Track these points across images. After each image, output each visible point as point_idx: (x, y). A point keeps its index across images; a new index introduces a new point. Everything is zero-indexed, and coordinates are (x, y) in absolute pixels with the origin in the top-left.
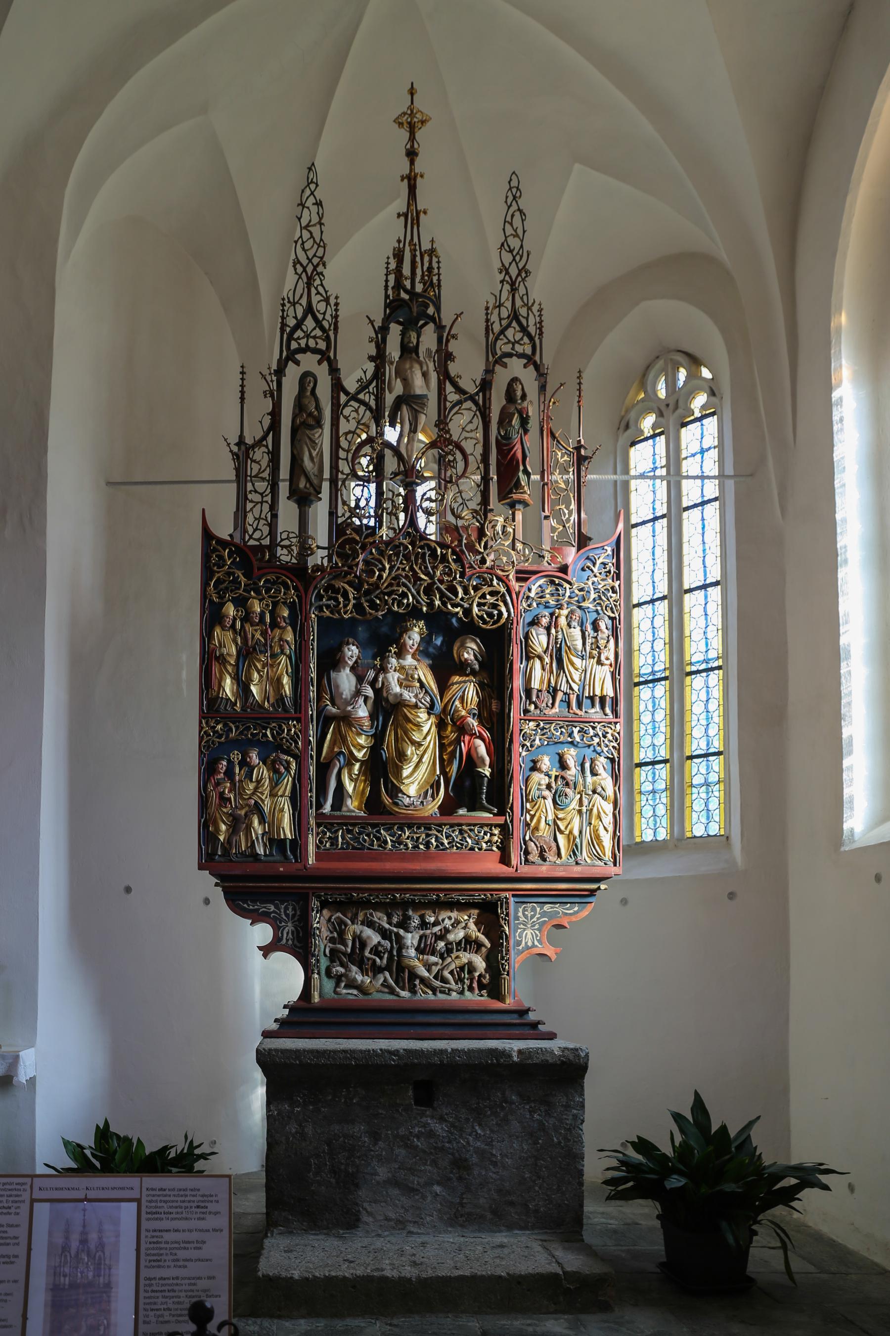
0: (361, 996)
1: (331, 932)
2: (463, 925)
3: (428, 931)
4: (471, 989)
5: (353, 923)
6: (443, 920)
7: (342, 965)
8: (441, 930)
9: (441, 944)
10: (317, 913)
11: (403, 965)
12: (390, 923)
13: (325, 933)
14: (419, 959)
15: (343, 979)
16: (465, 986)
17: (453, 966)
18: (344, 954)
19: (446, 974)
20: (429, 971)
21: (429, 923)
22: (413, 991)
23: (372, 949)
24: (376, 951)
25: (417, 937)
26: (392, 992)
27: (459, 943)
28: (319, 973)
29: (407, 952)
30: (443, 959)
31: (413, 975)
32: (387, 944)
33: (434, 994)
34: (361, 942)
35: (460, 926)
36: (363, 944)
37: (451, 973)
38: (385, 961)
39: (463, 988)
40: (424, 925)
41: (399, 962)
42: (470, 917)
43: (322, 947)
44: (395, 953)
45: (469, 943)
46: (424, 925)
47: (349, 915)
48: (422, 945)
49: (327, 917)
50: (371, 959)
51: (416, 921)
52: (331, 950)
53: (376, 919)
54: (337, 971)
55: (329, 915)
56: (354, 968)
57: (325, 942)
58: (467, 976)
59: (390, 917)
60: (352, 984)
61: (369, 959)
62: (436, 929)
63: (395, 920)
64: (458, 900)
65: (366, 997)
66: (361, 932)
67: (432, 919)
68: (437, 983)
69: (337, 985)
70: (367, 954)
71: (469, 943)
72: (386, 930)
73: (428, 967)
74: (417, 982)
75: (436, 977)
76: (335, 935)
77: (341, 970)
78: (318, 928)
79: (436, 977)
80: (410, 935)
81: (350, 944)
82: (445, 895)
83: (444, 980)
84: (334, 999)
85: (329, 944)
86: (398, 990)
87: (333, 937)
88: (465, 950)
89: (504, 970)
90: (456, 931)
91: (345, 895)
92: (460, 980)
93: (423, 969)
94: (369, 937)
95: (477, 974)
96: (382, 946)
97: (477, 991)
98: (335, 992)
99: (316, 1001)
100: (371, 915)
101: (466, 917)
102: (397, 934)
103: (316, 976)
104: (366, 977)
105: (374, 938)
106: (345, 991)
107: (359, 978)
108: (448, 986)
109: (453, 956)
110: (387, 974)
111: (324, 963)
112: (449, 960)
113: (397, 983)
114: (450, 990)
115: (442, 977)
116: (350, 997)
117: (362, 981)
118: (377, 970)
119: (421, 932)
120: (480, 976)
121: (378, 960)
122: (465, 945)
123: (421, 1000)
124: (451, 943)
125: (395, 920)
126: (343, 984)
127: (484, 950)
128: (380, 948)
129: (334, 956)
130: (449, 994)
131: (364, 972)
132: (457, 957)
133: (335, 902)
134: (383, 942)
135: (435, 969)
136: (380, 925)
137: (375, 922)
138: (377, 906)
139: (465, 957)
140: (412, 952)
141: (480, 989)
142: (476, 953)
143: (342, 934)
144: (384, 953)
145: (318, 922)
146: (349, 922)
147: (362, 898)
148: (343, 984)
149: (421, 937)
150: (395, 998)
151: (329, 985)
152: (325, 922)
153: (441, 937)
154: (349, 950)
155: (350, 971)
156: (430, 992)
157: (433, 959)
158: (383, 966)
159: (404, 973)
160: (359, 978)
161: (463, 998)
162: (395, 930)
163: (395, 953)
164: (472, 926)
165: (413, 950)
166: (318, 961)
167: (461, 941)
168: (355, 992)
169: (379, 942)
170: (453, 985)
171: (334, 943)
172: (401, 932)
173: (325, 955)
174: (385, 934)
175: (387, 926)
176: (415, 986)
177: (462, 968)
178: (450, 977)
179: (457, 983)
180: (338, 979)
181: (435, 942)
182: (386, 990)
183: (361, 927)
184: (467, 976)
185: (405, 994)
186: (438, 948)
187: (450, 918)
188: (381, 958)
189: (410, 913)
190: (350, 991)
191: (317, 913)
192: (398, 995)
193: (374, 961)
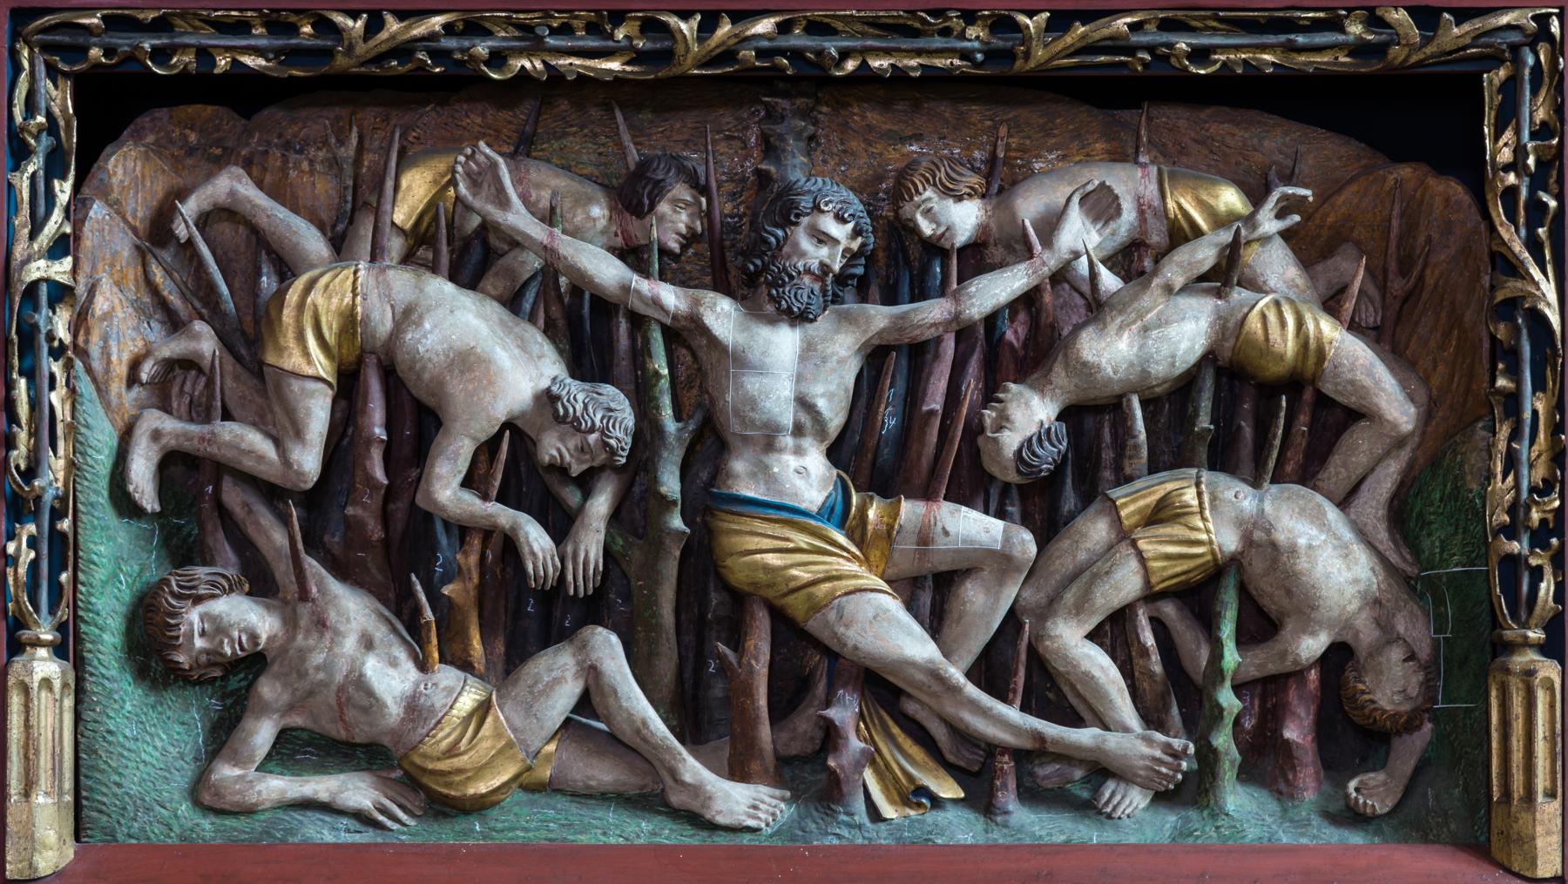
0: (406, 828)
1: (175, 324)
2: (1204, 254)
3: (934, 311)
4: (1265, 760)
5: (340, 245)
6: (1050, 225)
7: (259, 581)
8: (1028, 300)
9: (1031, 413)
10: (55, 168)
11: (738, 571)
12: (632, 255)
13: (122, 330)
14: (858, 532)
15: (268, 689)
16: (1223, 740)
17: (1125, 583)
18: (272, 493)
19: (1073, 643)
20: (935, 623)
21: (935, 249)
22: (812, 777)
23: (488, 448)
24: (513, 463)
25: (842, 350)
26: (653, 794)
27: (1172, 399)
28: (69, 646)
29: (763, 472)
30: (1048, 529)
31: (811, 657)
32: (610, 411)
33: (980, 799)
34: (394, 397)
35: (1175, 271)
36: (419, 421)
37: (1113, 632)
38: (591, 544)
39: (1208, 758)
40: (899, 260)
41: (702, 556)
42: (1256, 195)
43: (102, 437)
44: (671, 483)
45: (1252, 413)
46: (899, 260)
47: (323, 189)
48: (889, 420)
49: (139, 208)
50: (489, 533)
51: (828, 237)
52: (177, 466)
53: (518, 218)
54: (217, 629)
55: (158, 187)
56: (353, 610)
57: (129, 399)
58: (1231, 657)
59: (633, 195)
60: (333, 737)
61: (462, 531)
62: (995, 290)
63: (674, 219)
64: (1161, 56)
65: (445, 834)
66: (407, 316)
67: (965, 218)
68: (1007, 719)
69: (222, 736)
70: (447, 488)
71: (1252, 413)
72: (605, 306)
73: (933, 590)
74: (844, 713)
75: (990, 671)
76: (205, 342)
77: (253, 619)
78: (60, 293)
79: (990, 671)
80: (783, 343)
81: (318, 413)
82: (1060, 22)
83: (1053, 694)
84: (189, 849)
85: (154, 419)
86: (692, 768)
87: (187, 364)
88: (1222, 459)
89: (1523, 606)
90: (1152, 302)
91: (278, 25)
92: (1176, 695)
93: (892, 605)
94: (467, 361)
95: (1312, 646)
96: (574, 425)
97: (1308, 779)
98: (200, 792)
99: (46, 863)
100: (483, 178)
101: (1230, 198)
102: (686, 336)
103: (44, 666)
104: (447, 676)
105: (506, 366)
106: (278, 786)
107: (391, 678)
108: (1085, 736)
109: (1132, 501)
110: (608, 648)
111: (114, 563)
112: (1097, 531)
113: (694, 717)
114: (1101, 770)
115: (1040, 664)
116: (322, 832)
117: (414, 708)
118: (526, 619)
119: (879, 316)
120: (1339, 656)
121: (536, 538)
122: (1224, 413)
123: (870, 852)
124: (1115, 406)
125: (674, 219)
126: (262, 734)
127: (1358, 447)
128: (552, 447)
129: (194, 510)
130: (1089, 808)
131: (426, 633)
132: (1162, 513)
133: (201, 87)
134: (576, 393)
135: (984, 607)
136: (552, 268)
137: (516, 242)
138: (537, 113)
139: (1217, 513)
140: (807, 476)
141: (1335, 765)
142: (1307, 477)
143: (249, 337)
144: (586, 482)
145: (61, 247)
146: (313, 243)
147: (403, 50)
148: (262, 734)
149: (875, 357)
150: (669, 834)
151: (152, 742)
152: (123, 246)
153: (1028, 343)
154: (309, 461)
155: (321, 624)
156: (948, 790)
157: (971, 526)
158: (580, 583)
159: (737, 642)
160: (391, 678)
161: (1206, 832)
162: (671, 297)
163: (671, 483)
164: (1277, 266)
165: (815, 461)
166: (62, 550)
167: (1185, 385)
168: (358, 791)
169: (547, 399)
170: (1127, 736)
171: (200, 411)
172: (722, 316)
173: (123, 503)
174: (588, 331)
175: (607, 271)
176: (830, 736)
177: (1197, 593)
178: (1098, 664)
179: (1152, 718)
180: (233, 680)
181: (990, 394)
182: (603, 773)
183: (402, 282)
184: (1231, 657)
185: (742, 802)
186: (1011, 441)
187: (1101, 206)
188: (561, 525)
189: (795, 168)
190: (320, 786)
191: (55, 168)
192: (697, 820)
193: (509, 546)
